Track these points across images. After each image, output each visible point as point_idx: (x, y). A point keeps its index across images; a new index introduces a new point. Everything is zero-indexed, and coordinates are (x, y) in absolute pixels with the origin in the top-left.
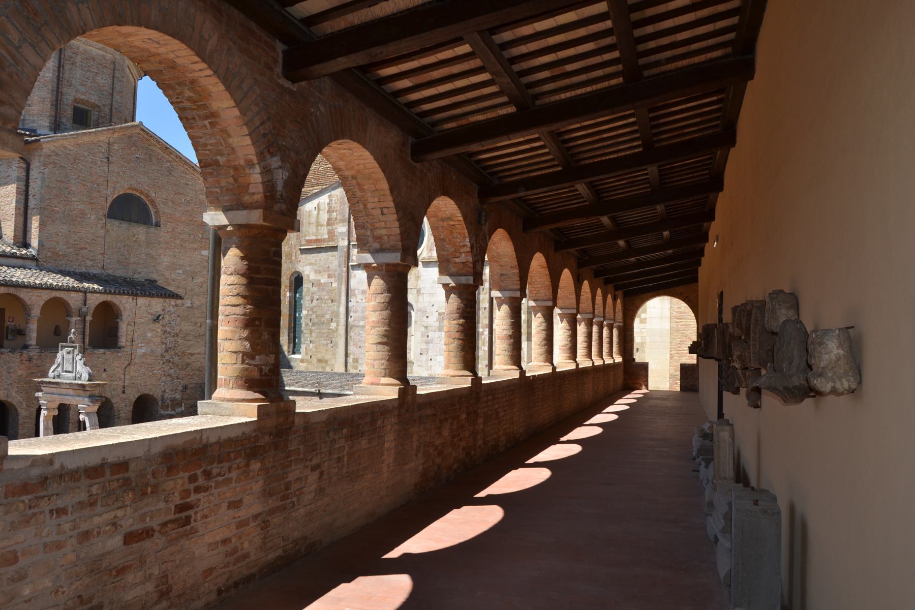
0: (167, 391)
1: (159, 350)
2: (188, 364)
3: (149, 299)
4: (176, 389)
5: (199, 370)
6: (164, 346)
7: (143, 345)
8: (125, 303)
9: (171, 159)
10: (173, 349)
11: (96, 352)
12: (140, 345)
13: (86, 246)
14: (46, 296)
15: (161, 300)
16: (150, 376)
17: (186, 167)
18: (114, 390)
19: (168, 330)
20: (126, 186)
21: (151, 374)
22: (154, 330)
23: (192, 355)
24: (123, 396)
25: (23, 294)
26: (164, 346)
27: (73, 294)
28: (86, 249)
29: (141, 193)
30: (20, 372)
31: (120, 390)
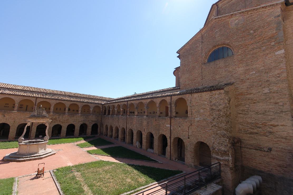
0: (215, 143)
1: (209, 119)
2: (271, 133)
3: (200, 93)
4: (222, 144)
5: (286, 139)
6: (212, 117)
7: (199, 116)
8: (187, 97)
9: (237, 18)
10: (217, 119)
11: (176, 119)
12: (196, 116)
13: (196, 79)
14: (160, 100)
15: (209, 92)
16: (204, 133)
17: (249, 13)
18: (184, 136)
19: (214, 107)
20: (211, 47)
21: (204, 131)
22: (204, 109)
23: (275, 126)
24: (189, 139)
25: (155, 100)
26: (212, 117)
27: (168, 98)
28: (195, 79)
29: (222, 45)
30: (154, 124)
31: (187, 138)
